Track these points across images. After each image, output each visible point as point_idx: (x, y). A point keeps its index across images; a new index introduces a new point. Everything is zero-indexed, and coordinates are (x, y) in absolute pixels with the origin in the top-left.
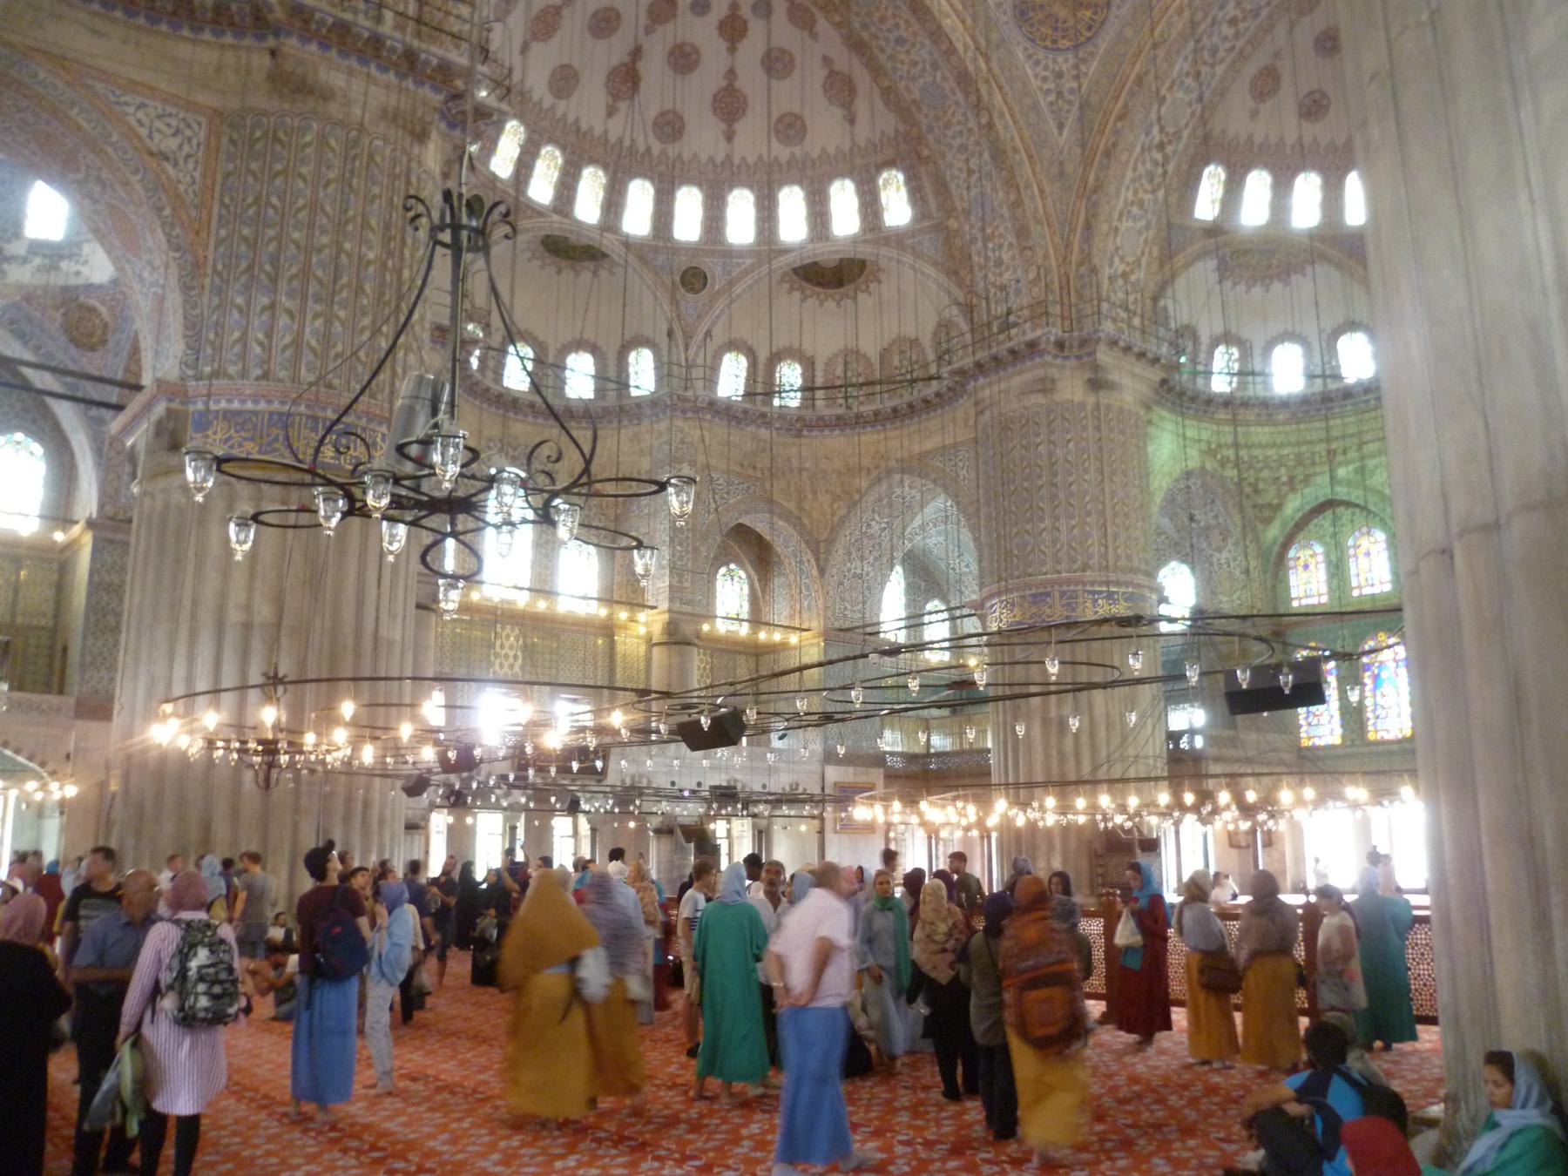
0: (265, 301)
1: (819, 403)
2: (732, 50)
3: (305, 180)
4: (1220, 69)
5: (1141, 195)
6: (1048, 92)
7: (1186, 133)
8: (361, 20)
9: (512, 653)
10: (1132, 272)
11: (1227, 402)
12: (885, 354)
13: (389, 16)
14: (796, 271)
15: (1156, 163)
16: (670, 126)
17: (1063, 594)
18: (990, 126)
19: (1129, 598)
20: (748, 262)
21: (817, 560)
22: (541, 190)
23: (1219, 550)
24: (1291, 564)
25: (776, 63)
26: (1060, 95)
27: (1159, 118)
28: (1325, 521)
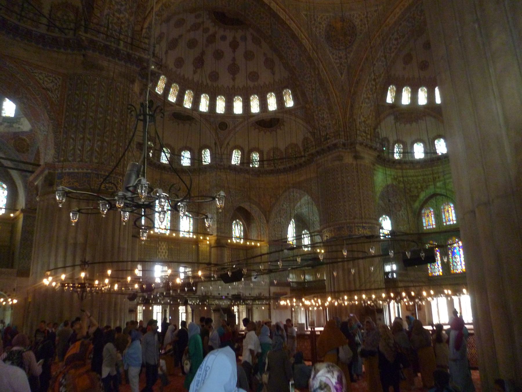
0: (81, 136)
1: (265, 166)
2: (234, 51)
3: (94, 97)
4: (393, 55)
5: (369, 95)
6: (337, 63)
7: (383, 75)
8: (113, 44)
9: (164, 251)
10: (367, 120)
11: (399, 162)
12: (286, 149)
13: (122, 43)
14: (257, 122)
15: (372, 85)
16: (214, 76)
17: (348, 227)
18: (319, 74)
19: (370, 228)
20: (241, 120)
21: (266, 218)
22: (172, 99)
23: (399, 211)
24: (423, 215)
25: (249, 56)
26: (341, 64)
27: (373, 71)
28: (433, 201)
